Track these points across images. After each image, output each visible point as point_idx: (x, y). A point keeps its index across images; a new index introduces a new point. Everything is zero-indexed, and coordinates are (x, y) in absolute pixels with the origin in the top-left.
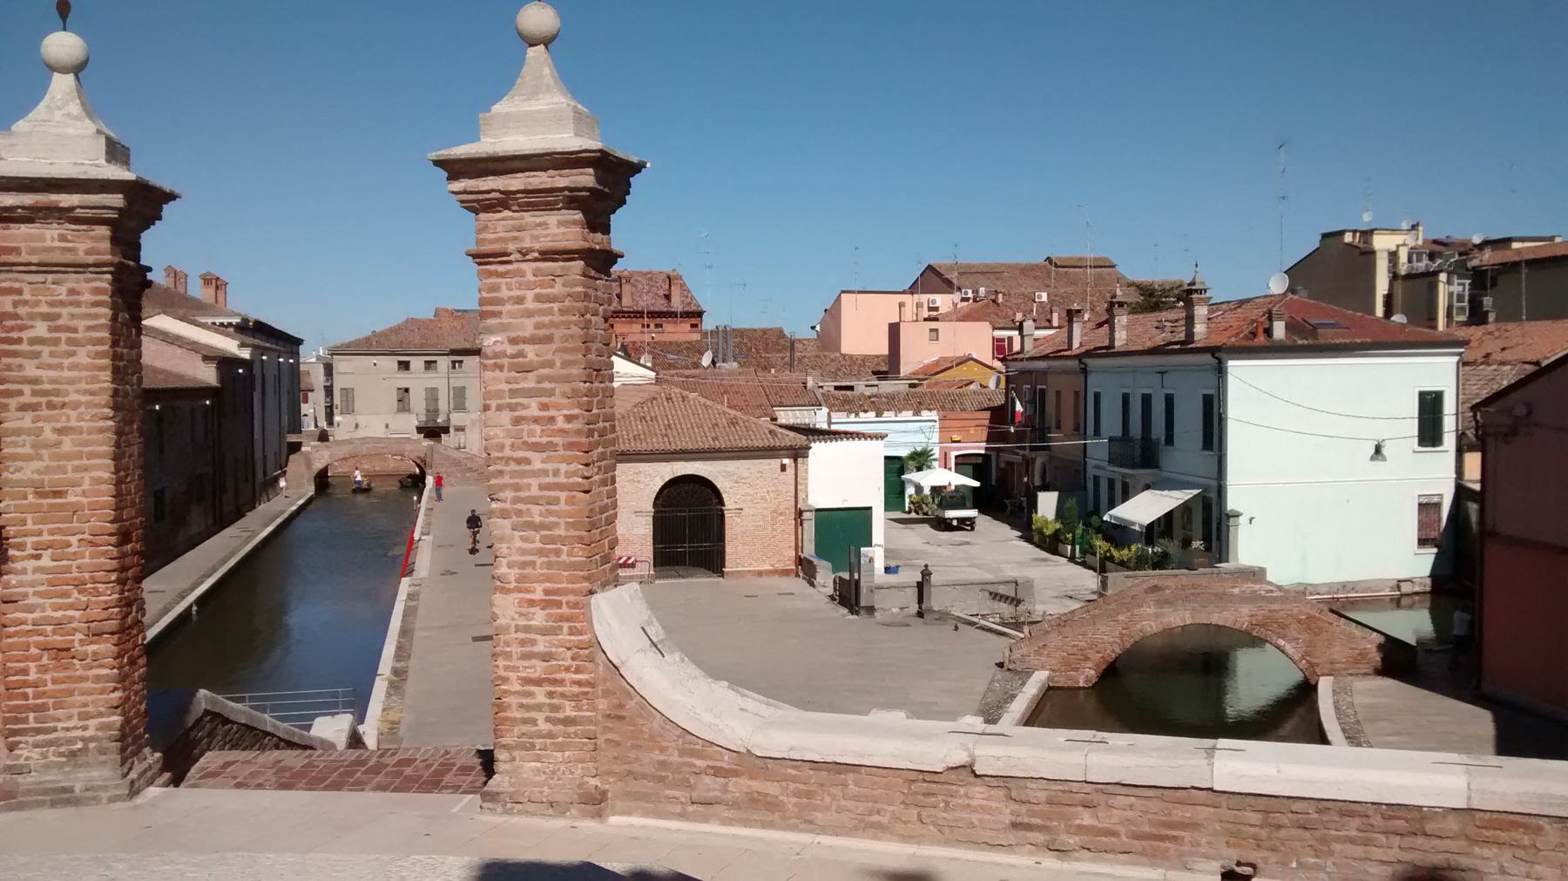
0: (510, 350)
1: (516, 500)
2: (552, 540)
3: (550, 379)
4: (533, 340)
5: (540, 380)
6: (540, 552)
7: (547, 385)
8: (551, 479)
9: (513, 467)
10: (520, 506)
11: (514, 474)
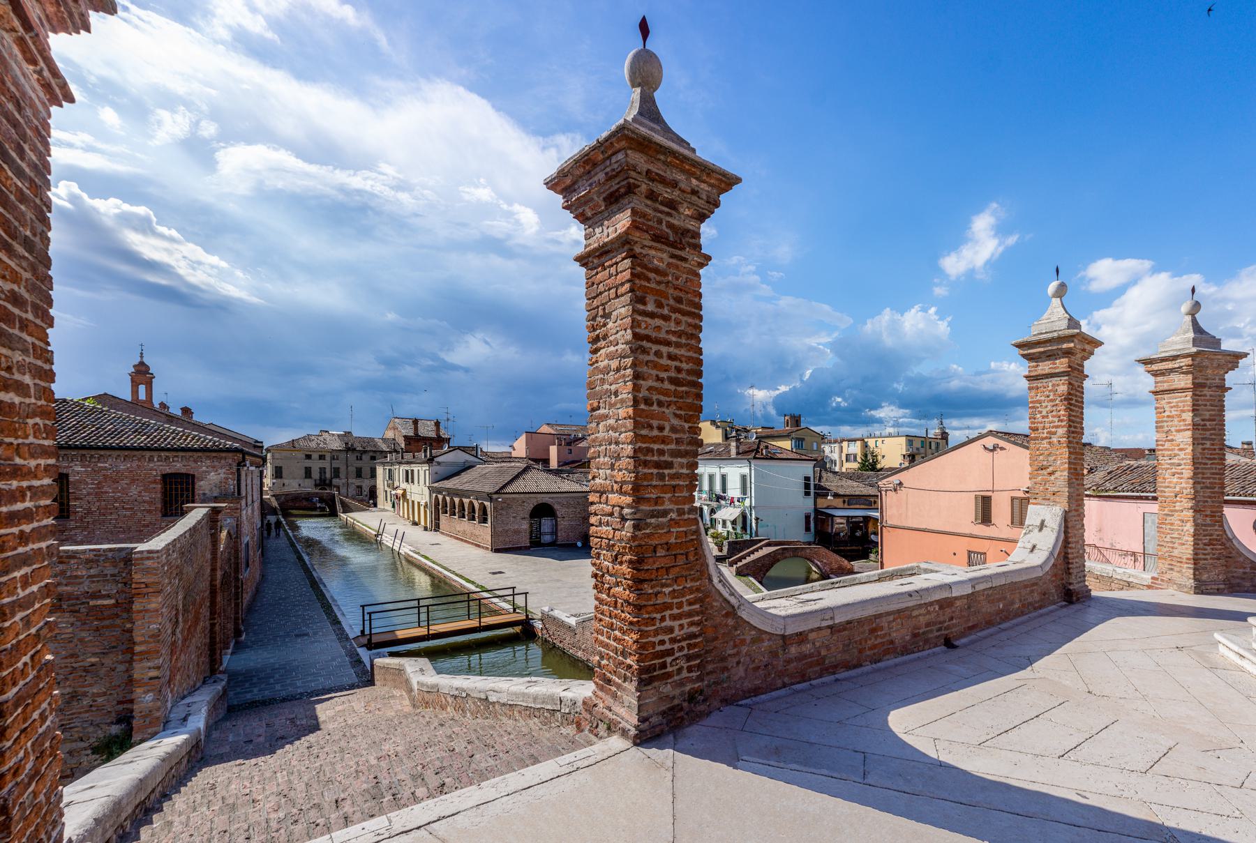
0: (1202, 423)
1: (1203, 478)
2: (1214, 493)
3: (1215, 435)
4: (1209, 420)
5: (1211, 434)
6: (1210, 497)
7: (1213, 437)
8: (1214, 471)
9: (1202, 466)
10: (1204, 481)
11: (1202, 469)
